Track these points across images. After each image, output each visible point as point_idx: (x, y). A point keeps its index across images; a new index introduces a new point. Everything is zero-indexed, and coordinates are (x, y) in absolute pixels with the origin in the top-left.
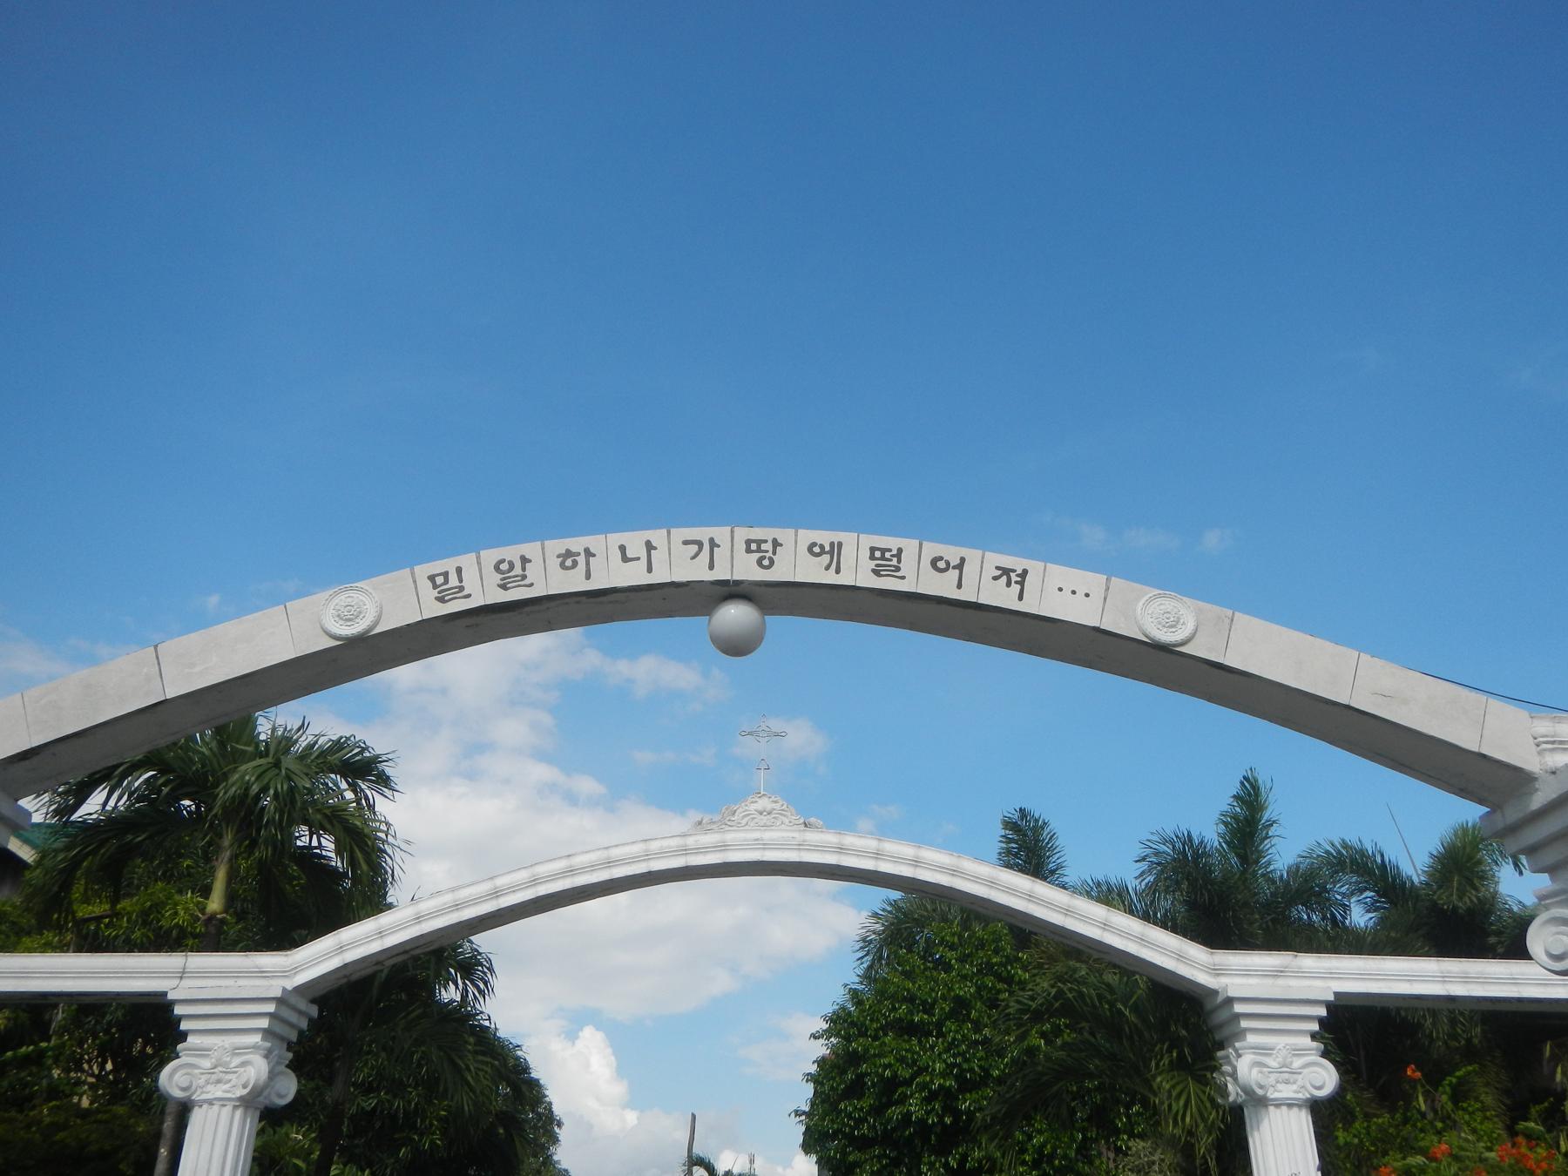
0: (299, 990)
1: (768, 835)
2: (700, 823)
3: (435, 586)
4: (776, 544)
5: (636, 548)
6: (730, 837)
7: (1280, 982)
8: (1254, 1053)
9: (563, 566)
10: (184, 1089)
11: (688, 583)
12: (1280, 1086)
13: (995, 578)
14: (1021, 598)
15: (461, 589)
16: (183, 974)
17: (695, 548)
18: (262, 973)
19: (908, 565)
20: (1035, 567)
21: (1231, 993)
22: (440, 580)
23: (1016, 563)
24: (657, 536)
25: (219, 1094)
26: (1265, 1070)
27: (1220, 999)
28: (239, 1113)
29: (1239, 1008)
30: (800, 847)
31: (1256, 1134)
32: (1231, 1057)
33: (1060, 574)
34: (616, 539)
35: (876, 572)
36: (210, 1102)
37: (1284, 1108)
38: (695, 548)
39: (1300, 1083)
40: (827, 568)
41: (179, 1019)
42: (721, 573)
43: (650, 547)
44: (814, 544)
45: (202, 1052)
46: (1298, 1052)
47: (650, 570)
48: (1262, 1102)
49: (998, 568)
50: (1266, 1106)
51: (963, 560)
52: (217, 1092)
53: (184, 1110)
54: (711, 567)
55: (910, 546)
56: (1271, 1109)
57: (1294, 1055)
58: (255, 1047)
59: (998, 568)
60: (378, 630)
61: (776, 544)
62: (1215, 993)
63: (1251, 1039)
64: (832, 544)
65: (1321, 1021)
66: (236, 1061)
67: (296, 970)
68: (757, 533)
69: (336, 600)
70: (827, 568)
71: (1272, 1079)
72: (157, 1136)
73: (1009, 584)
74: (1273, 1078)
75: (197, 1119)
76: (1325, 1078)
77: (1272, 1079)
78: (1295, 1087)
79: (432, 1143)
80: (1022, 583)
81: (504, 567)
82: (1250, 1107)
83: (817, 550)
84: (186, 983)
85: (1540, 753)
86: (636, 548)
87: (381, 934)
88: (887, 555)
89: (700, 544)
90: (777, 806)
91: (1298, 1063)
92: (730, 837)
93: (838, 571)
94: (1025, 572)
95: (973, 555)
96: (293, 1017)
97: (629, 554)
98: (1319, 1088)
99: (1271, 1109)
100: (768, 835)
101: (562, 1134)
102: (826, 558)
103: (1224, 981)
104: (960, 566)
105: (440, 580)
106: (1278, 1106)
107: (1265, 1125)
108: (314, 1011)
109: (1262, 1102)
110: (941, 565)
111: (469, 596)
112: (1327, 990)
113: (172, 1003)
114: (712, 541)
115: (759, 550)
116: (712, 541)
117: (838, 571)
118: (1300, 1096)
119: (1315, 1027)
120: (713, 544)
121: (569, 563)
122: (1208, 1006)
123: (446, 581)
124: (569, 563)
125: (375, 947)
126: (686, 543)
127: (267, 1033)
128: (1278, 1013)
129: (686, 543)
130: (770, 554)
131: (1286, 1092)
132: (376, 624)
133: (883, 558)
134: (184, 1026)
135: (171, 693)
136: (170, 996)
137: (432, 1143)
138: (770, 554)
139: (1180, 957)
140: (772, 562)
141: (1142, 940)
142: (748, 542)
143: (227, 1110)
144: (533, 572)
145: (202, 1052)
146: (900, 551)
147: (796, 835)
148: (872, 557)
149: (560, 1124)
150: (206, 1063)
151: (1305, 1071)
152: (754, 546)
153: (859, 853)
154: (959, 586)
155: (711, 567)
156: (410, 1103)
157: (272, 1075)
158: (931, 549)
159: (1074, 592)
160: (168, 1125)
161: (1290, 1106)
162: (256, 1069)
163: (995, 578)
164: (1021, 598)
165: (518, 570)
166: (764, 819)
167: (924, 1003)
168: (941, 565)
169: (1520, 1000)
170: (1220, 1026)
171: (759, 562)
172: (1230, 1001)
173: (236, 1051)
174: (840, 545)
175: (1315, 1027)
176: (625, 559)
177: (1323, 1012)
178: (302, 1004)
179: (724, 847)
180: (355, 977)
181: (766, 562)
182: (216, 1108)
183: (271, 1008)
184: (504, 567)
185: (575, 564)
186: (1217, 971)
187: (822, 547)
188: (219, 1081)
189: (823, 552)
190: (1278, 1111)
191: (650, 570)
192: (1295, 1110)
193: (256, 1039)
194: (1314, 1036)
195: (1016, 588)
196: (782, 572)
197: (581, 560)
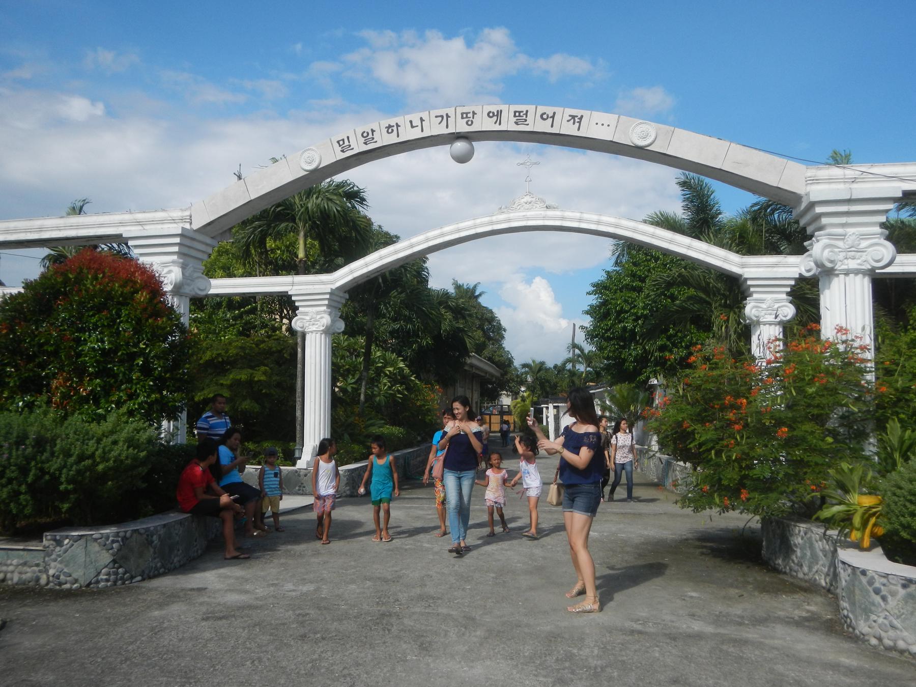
0: (338, 288)
1: (529, 214)
2: (501, 208)
3: (340, 146)
4: (474, 113)
5: (417, 122)
6: (512, 215)
7: (775, 269)
9: (388, 132)
10: (301, 328)
11: (438, 135)
13: (568, 121)
14: (579, 129)
15: (350, 146)
16: (293, 284)
17: (440, 118)
18: (323, 283)
19: (530, 119)
20: (586, 113)
22: (341, 143)
23: (577, 112)
24: (425, 115)
25: (315, 329)
28: (323, 336)
29: (749, 283)
30: (544, 218)
33: (599, 116)
34: (408, 117)
35: (516, 123)
36: (312, 332)
38: (440, 118)
40: (496, 123)
41: (294, 302)
42: (451, 130)
43: (422, 120)
44: (490, 112)
45: (306, 314)
47: (422, 131)
48: (758, 323)
49: (570, 116)
51: (554, 113)
52: (314, 328)
53: (304, 336)
54: (447, 127)
55: (531, 108)
58: (324, 311)
59: (570, 116)
60: (321, 166)
61: (474, 113)
63: (755, 296)
64: (498, 111)
65: (792, 286)
66: (319, 317)
67: (336, 281)
68: (465, 110)
69: (304, 155)
70: (496, 123)
71: (763, 313)
72: (296, 344)
73: (574, 123)
75: (308, 337)
77: (763, 313)
79: (427, 342)
80: (580, 123)
81: (365, 135)
83: (491, 115)
84: (295, 287)
85: (806, 185)
86: (417, 122)
87: (367, 265)
88: (521, 114)
89: (442, 117)
90: (534, 199)
92: (512, 215)
93: (500, 124)
94: (582, 116)
95: (559, 110)
96: (338, 299)
97: (414, 124)
98: (785, 316)
100: (529, 214)
101: (506, 335)
102: (495, 118)
103: (746, 270)
104: (553, 117)
105: (341, 143)
106: (765, 325)
108: (347, 296)
109: (758, 323)
110: (545, 116)
111: (353, 149)
112: (794, 273)
113: (291, 296)
114: (447, 115)
115: (467, 117)
116: (447, 115)
117: (500, 124)
120: (448, 116)
121: (390, 131)
123: (344, 143)
124: (390, 131)
125: (365, 271)
126: (436, 117)
127: (328, 306)
128: (770, 284)
129: (436, 117)
130: (471, 119)
132: (320, 164)
133: (520, 116)
134: (297, 304)
135: (253, 198)
136: (289, 293)
137: (427, 342)
138: (471, 119)
140: (472, 122)
141: (707, 253)
142: (462, 114)
143: (318, 335)
144: (377, 136)
145: (306, 314)
146: (527, 111)
147: (542, 213)
148: (515, 116)
149: (505, 330)
150: (308, 318)
152: (465, 116)
153: (572, 220)
154: (552, 126)
155: (447, 127)
156: (414, 326)
157: (333, 321)
158: (541, 109)
159: (603, 125)
160: (299, 340)
161: (770, 324)
162: (326, 320)
163: (568, 121)
164: (579, 129)
165: (370, 136)
166: (527, 206)
167: (640, 277)
168: (545, 116)
169: (903, 273)
171: (467, 123)
172: (746, 279)
173: (318, 313)
174: (501, 111)
176: (412, 127)
177: (793, 283)
178: (341, 294)
179: (509, 220)
180: (360, 282)
181: (470, 123)
182: (314, 334)
183: (328, 296)
184: (365, 135)
185: (393, 130)
186: (743, 266)
187: (493, 113)
188: (313, 324)
189: (494, 115)
191: (422, 131)
193: (324, 308)
195: (577, 125)
196: (475, 128)
197: (395, 128)
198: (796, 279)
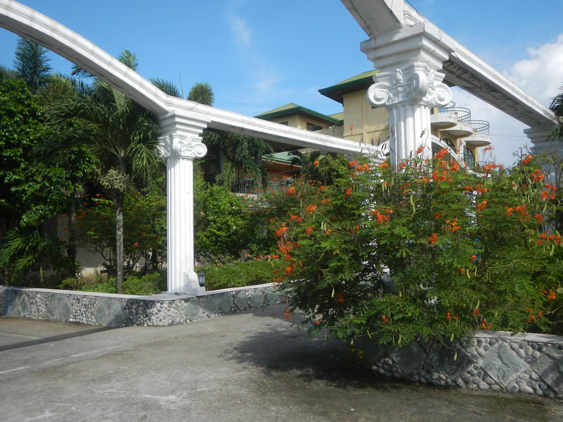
7: (191, 112)
8: (180, 138)
12: (186, 152)
21: (176, 113)
26: (182, 145)
27: (168, 115)
29: (177, 120)
31: (173, 169)
32: (167, 139)
37: (186, 160)
39: (193, 151)
46: (194, 140)
50: (179, 159)
56: (181, 160)
57: (193, 141)
62: (167, 112)
63: (178, 132)
65: (204, 129)
74: (185, 147)
76: (202, 151)
78: (191, 153)
82: (171, 159)
91: (194, 144)
99: (181, 160)
106: (183, 159)
107: (177, 166)
118: (192, 156)
119: (201, 131)
122: (161, 117)
128: (190, 123)
131: (188, 154)
139: (156, 95)
151: (196, 147)
161: (188, 159)
170: (165, 127)
172: (174, 116)
175: (201, 131)
186: (169, 104)
190: (183, 161)
192: (189, 161)
194: (200, 135)
198: (208, 123)
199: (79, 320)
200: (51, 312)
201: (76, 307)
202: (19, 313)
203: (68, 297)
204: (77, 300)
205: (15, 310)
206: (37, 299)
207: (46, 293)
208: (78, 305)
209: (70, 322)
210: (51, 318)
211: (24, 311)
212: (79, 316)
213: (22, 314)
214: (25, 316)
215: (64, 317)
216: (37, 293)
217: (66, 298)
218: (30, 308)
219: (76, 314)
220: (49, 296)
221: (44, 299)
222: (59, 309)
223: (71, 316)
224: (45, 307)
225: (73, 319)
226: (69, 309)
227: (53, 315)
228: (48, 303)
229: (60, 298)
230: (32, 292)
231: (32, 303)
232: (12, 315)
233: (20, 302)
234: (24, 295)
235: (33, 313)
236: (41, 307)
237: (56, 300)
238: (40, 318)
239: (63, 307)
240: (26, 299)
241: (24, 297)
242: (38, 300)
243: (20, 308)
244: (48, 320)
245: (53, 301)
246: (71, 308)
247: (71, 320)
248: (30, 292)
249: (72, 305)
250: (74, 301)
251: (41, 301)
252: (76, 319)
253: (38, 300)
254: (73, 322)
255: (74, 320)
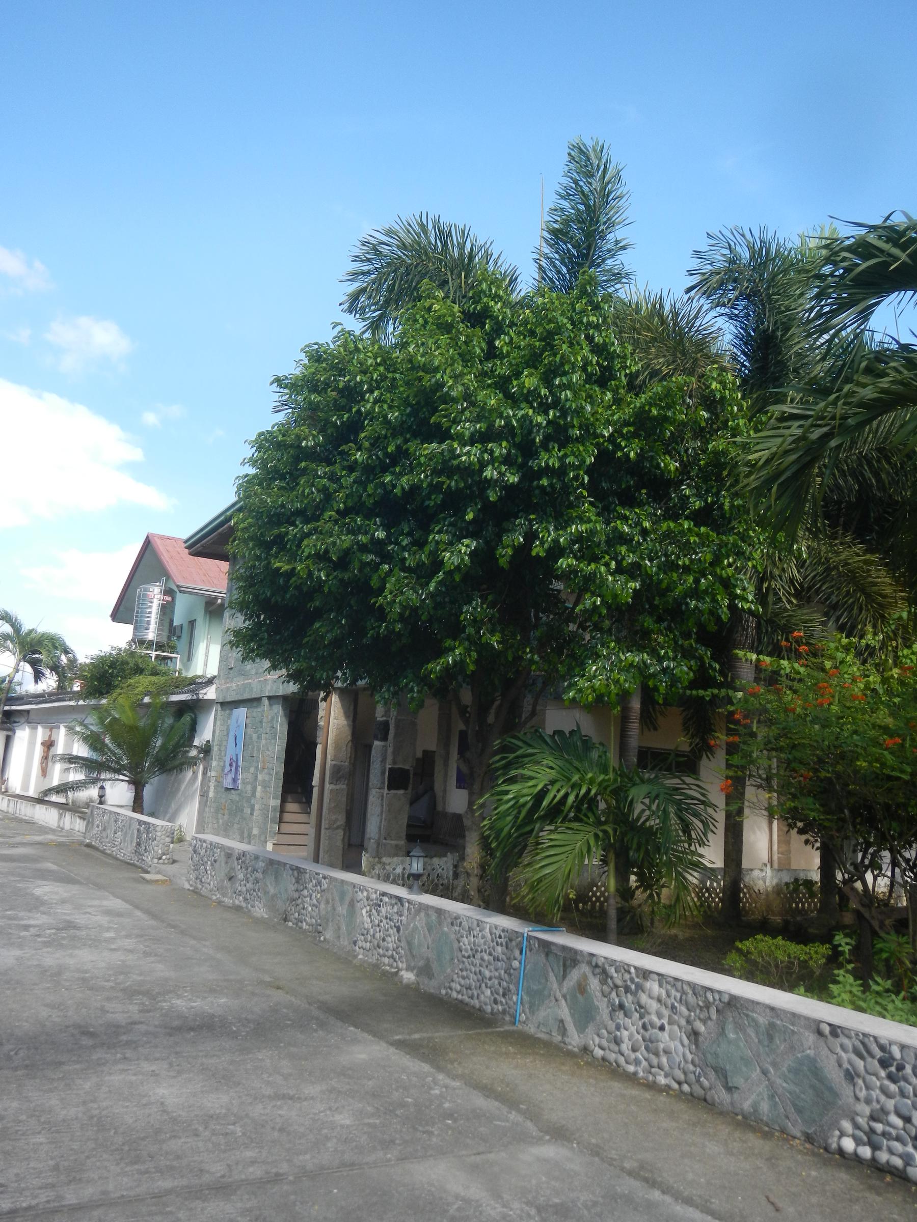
199: (898, 1162)
200: (722, 1073)
201: (877, 1093)
202: (563, 1031)
203: (820, 1033)
204: (884, 1064)
205: (542, 1014)
206: (644, 998)
207: (693, 986)
208: (893, 1087)
209: (841, 1151)
210: (721, 1095)
211: (581, 1028)
212: (898, 1139)
213: (575, 1040)
214: (585, 1049)
215: (794, 1115)
216: (646, 974)
217: (810, 1038)
218: (612, 1026)
219: (879, 1127)
220: (708, 1006)
221: (684, 1010)
222: (765, 1073)
223: (847, 1125)
224: (686, 1041)
225: (858, 1142)
226: (836, 1095)
227: (729, 1089)
228: (701, 1028)
229: (772, 1025)
230: (624, 968)
231: (621, 1006)
232: (531, 1029)
233: (565, 990)
234: (585, 968)
235: (625, 1047)
236: (665, 1036)
237: (751, 1032)
238: (662, 1080)
239: (796, 1071)
240: (594, 984)
241: (585, 977)
242: (653, 1005)
243: (564, 1012)
244: (702, 1102)
245: (730, 1027)
246: (846, 1091)
247: (848, 1144)
248: (613, 962)
249: (851, 1076)
250: (860, 1064)
251: (666, 1013)
252: (875, 1147)
253: (653, 1005)
254: (856, 1157)
255: (866, 1152)
